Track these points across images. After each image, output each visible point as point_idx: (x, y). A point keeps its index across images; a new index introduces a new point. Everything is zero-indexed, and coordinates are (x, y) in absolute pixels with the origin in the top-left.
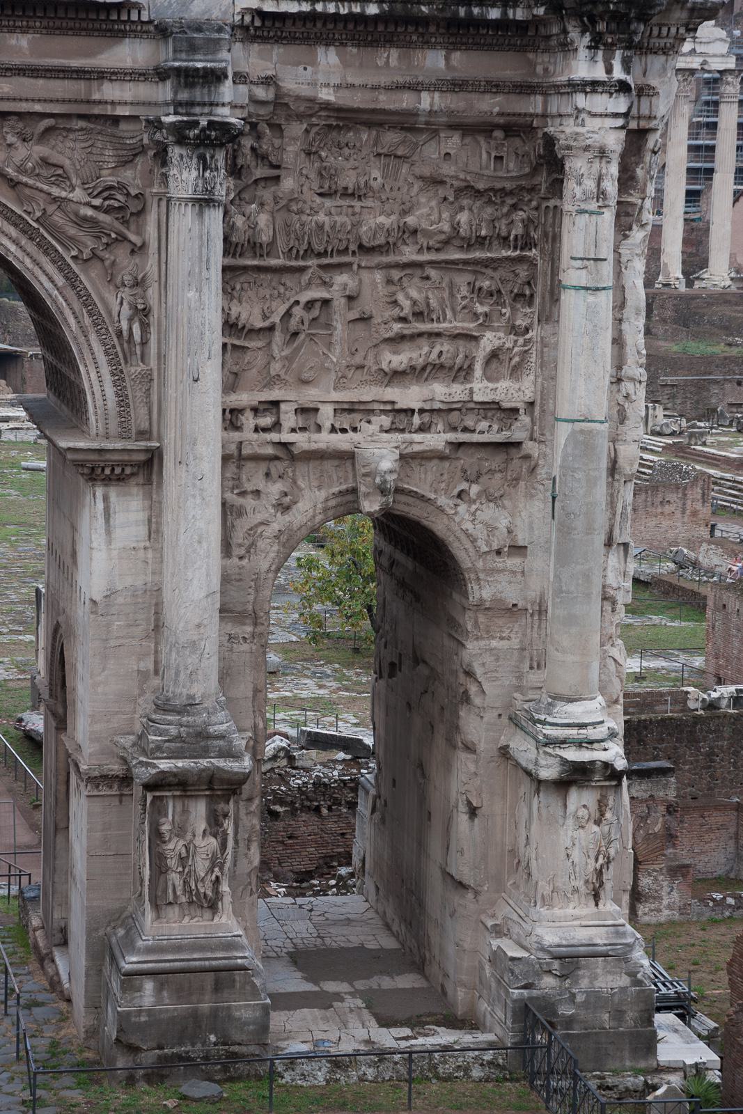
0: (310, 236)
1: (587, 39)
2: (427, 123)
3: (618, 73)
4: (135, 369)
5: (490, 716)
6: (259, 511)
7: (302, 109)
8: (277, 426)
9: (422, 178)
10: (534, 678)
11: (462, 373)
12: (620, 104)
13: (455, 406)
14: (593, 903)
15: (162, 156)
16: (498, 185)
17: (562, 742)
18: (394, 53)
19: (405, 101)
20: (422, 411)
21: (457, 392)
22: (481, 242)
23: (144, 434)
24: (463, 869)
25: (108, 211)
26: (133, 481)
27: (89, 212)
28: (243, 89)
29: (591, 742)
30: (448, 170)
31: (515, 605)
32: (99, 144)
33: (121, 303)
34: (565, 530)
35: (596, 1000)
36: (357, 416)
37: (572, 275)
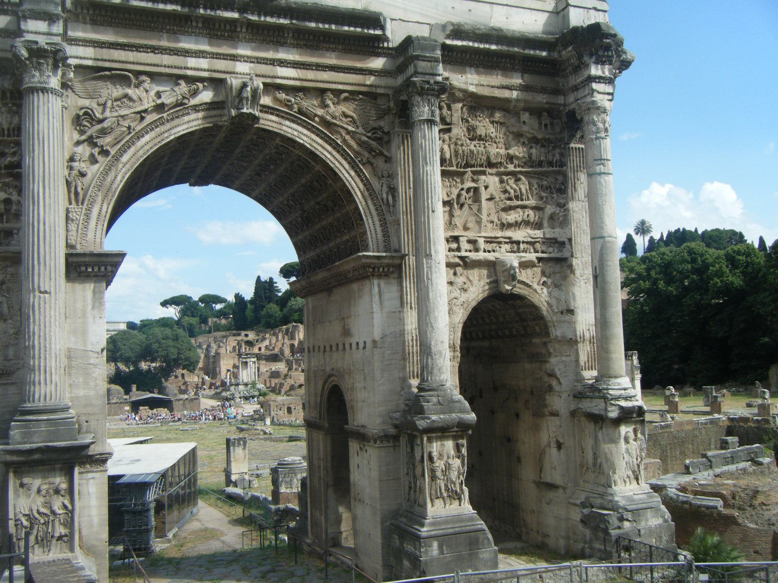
0: (467, 157)
1: (594, 59)
2: (515, 107)
3: (607, 74)
5: (564, 395)
7: (461, 95)
8: (458, 249)
9: (512, 133)
13: (537, 240)
14: (635, 482)
16: (547, 137)
17: (618, 398)
20: (523, 242)
22: (540, 164)
25: (373, 140)
26: (392, 276)
27: (366, 139)
29: (631, 397)
31: (571, 339)
32: (369, 108)
33: (382, 186)
35: (651, 531)
36: (494, 245)
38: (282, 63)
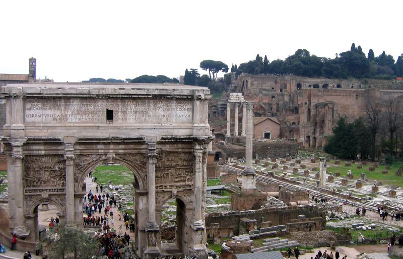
3: (201, 148)
4: (145, 182)
5: (189, 222)
6: (160, 198)
8: (162, 188)
10: (194, 217)
11: (185, 181)
12: (202, 151)
15: (148, 158)
17: (197, 225)
18: (175, 145)
19: (177, 150)
21: (184, 183)
22: (186, 166)
23: (146, 190)
24: (186, 240)
28: (158, 150)
30: (182, 158)
34: (197, 200)
37: (197, 171)
38: (120, 149)
